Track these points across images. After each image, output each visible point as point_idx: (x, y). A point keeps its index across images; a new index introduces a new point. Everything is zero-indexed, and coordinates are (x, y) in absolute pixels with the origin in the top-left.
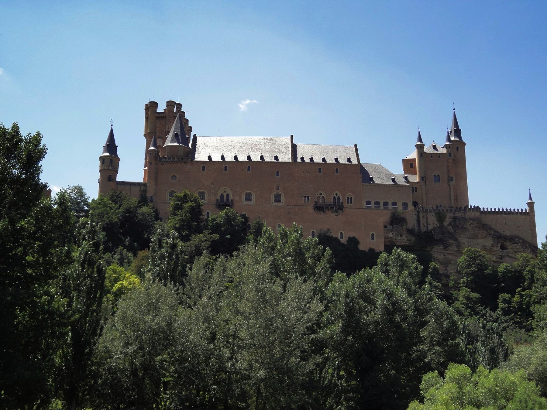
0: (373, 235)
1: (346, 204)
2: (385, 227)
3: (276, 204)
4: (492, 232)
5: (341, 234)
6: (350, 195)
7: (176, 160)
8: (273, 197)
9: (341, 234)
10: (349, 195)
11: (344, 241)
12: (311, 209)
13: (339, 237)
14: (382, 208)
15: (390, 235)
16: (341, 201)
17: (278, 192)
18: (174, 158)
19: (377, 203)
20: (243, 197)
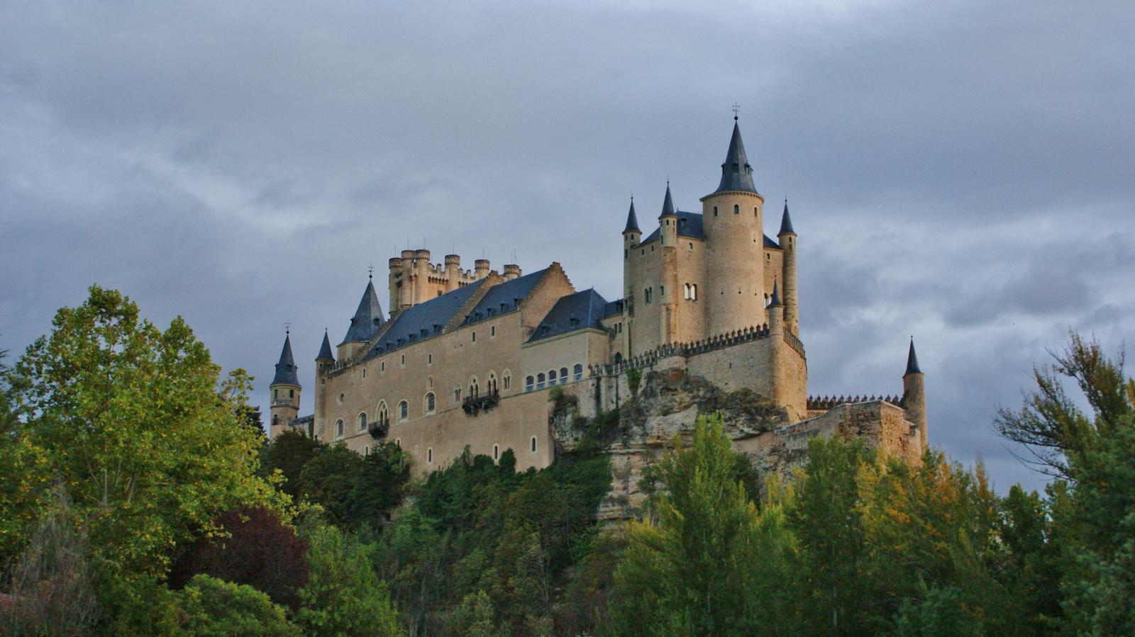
0: (534, 439)
1: (503, 392)
2: (551, 421)
3: (428, 414)
4: (701, 393)
5: (496, 447)
6: (507, 373)
8: (426, 402)
9: (496, 447)
10: (507, 373)
11: (497, 462)
12: (461, 412)
13: (493, 457)
14: (546, 385)
15: (557, 436)
17: (429, 390)
19: (541, 377)
20: (400, 409)
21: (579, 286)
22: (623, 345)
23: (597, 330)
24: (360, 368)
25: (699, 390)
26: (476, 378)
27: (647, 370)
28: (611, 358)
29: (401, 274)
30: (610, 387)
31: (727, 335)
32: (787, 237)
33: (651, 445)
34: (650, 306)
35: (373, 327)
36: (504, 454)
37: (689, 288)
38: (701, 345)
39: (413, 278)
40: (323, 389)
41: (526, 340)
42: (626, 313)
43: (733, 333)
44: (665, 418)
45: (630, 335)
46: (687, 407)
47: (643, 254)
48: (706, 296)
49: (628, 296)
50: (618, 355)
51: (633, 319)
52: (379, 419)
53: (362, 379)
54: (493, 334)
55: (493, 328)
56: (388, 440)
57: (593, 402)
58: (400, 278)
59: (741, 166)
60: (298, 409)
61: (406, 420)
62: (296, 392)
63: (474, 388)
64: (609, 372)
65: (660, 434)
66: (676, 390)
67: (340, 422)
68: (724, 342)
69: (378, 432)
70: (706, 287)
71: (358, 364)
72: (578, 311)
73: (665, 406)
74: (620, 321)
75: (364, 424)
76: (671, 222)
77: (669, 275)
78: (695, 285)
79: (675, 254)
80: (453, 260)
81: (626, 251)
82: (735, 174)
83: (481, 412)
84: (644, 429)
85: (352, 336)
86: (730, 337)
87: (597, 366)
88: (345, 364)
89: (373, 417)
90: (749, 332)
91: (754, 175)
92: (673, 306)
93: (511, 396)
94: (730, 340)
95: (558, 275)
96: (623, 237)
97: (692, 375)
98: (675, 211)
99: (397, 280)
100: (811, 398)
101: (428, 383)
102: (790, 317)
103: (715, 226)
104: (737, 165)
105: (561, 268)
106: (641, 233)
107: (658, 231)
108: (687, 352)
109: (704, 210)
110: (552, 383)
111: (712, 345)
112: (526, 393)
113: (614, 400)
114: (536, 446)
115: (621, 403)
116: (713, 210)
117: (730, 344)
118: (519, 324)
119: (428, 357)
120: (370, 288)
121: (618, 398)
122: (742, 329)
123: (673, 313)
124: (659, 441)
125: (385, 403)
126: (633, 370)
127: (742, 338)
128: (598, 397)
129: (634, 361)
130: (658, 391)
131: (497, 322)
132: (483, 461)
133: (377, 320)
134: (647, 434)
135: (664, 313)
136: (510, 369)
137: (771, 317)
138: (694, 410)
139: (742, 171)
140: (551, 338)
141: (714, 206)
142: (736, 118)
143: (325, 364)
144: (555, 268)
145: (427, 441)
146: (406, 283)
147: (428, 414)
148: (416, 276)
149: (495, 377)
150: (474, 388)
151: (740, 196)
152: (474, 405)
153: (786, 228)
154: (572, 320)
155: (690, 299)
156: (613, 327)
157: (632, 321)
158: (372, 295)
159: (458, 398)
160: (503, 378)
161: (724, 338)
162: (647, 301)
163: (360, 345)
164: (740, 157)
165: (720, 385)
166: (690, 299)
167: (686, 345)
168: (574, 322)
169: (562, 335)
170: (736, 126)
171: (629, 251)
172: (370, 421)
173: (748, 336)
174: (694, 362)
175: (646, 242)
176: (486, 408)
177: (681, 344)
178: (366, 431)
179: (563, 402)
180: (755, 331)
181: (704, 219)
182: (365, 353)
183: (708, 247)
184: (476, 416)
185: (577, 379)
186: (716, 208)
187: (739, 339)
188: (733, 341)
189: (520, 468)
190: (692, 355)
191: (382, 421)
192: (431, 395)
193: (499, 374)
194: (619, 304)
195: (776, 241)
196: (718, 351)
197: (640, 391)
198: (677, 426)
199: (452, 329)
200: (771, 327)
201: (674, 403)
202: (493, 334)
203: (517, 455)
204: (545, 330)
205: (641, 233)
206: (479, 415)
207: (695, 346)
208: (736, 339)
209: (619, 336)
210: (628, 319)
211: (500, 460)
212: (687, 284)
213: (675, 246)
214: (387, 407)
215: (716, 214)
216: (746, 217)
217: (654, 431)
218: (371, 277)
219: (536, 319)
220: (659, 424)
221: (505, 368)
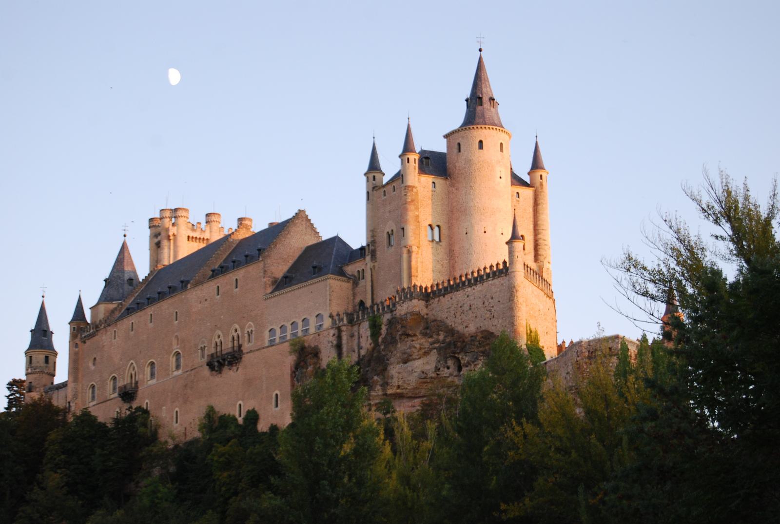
0: (277, 395)
1: (246, 347)
2: (294, 374)
3: (176, 373)
4: (441, 337)
5: (240, 405)
6: (250, 326)
7: (92, 331)
9: (240, 405)
10: (250, 326)
11: (240, 420)
12: (206, 371)
14: (288, 338)
16: (240, 343)
17: (176, 348)
18: (90, 330)
20: (148, 370)
21: (325, 235)
22: (366, 291)
23: (337, 277)
24: (111, 330)
25: (438, 335)
26: (220, 333)
27: (388, 316)
28: (354, 306)
29: (159, 234)
30: (352, 336)
31: (466, 275)
32: (538, 173)
33: (391, 394)
34: (392, 250)
35: (127, 287)
36: (248, 412)
37: (432, 229)
38: (441, 287)
39: (172, 237)
40: (76, 354)
41: (269, 290)
42: (368, 258)
43: (473, 273)
44: (406, 365)
45: (372, 281)
46: (426, 353)
47: (385, 195)
48: (451, 237)
49: (370, 240)
50: (362, 303)
51: (376, 264)
52: (129, 382)
53: (114, 341)
54: (237, 287)
55: (237, 280)
56: (135, 405)
57: (333, 354)
58: (159, 238)
59: (485, 99)
60: (54, 375)
61: (154, 381)
62: (51, 358)
63: (219, 344)
64: (351, 322)
65: (400, 383)
66: (415, 335)
67: (93, 387)
68: (464, 283)
69: (128, 395)
70: (450, 227)
71: (109, 325)
72: (326, 258)
73: (405, 353)
74: (363, 268)
75: (114, 389)
76: (412, 160)
77: (411, 215)
78: (438, 226)
79: (417, 193)
80: (213, 218)
81: (368, 193)
82: (479, 108)
83: (225, 369)
84: (384, 378)
85: (105, 298)
86: (470, 277)
87: (338, 315)
88: (97, 327)
89: (124, 381)
90: (488, 271)
91: (501, 109)
92: (414, 249)
93: (254, 351)
94: (469, 280)
95: (303, 223)
96: (365, 178)
97: (433, 317)
98: (418, 150)
99: (156, 240)
100: (564, 342)
101: (174, 342)
102: (541, 258)
103: (457, 163)
104: (481, 98)
105: (307, 216)
106: (384, 174)
107: (399, 172)
108: (427, 296)
109: (448, 147)
110: (295, 334)
111: (452, 287)
112: (268, 347)
113: (356, 351)
114: (279, 402)
115: (363, 352)
116: (456, 146)
117: (470, 285)
118: (262, 274)
119: (175, 314)
120: (124, 248)
121: (360, 348)
122: (482, 268)
123: (414, 256)
124: (398, 391)
125: (134, 364)
126: (375, 317)
127: (482, 277)
128: (339, 347)
129: (375, 308)
130: (398, 338)
131: (240, 274)
132: (227, 421)
133: (131, 280)
134: (387, 383)
135: (405, 256)
136: (253, 322)
137: (511, 253)
138: (433, 357)
139: (486, 104)
140: (293, 288)
141: (458, 141)
142: (480, 50)
143: (78, 327)
144: (300, 216)
145: (173, 402)
146: (165, 243)
147: (176, 373)
148: (174, 235)
149: (239, 332)
150: (219, 344)
151: (484, 131)
152: (218, 362)
153: (536, 164)
154: (314, 267)
155: (433, 240)
156: (356, 274)
157: (374, 266)
158: (126, 254)
159: (203, 356)
160: (246, 332)
161: (464, 279)
162: (390, 244)
163: (112, 306)
164: (484, 90)
165: (460, 328)
166: (433, 240)
167: (426, 289)
168: (317, 270)
169: (305, 284)
170: (480, 59)
171: (371, 193)
172: (120, 383)
173: (488, 275)
174: (433, 305)
175: (387, 184)
176: (231, 364)
177: (421, 287)
178: (116, 395)
179: (305, 354)
180: (495, 269)
181: (448, 156)
182: (117, 314)
183: (452, 185)
184: (220, 373)
185: (319, 329)
186: (459, 144)
187: (479, 279)
188: (473, 282)
189: (263, 427)
190: (432, 298)
191: (131, 383)
192: (178, 354)
193: (242, 328)
194: (362, 249)
195: (527, 179)
196: (459, 293)
197: (380, 340)
198: (416, 374)
199: (198, 283)
200: (510, 264)
201: (413, 350)
202: (237, 287)
203: (261, 413)
204: (288, 280)
205: (384, 174)
206: (223, 372)
207: (435, 288)
208: (476, 279)
209: (362, 283)
210: (370, 265)
211: (243, 419)
212: (430, 225)
213: (416, 184)
214: (136, 368)
215: (460, 151)
216: (491, 151)
217: (394, 380)
218: (125, 236)
219: (280, 269)
220: (399, 373)
221: (249, 321)
